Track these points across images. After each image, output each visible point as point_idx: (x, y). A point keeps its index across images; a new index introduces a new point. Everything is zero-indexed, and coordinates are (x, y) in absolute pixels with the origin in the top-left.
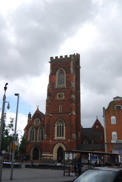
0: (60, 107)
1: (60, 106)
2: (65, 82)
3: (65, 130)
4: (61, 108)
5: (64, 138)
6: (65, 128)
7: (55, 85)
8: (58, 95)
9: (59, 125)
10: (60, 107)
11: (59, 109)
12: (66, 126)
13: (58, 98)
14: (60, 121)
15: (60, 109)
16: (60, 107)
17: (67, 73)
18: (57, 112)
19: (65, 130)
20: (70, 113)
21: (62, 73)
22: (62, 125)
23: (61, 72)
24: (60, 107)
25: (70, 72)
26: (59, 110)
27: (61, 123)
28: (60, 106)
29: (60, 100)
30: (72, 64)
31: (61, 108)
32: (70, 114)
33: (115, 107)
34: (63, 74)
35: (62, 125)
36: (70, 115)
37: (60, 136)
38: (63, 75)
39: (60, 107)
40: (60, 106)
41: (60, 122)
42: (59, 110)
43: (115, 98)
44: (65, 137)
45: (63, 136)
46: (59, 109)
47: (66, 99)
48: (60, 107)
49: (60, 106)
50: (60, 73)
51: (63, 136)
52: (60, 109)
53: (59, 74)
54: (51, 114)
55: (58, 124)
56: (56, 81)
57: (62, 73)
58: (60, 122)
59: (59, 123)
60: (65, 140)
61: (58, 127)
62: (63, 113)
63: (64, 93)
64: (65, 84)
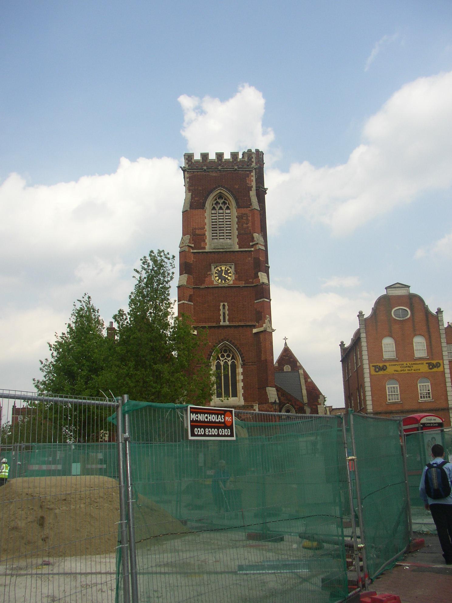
0: (224, 309)
1: (222, 304)
2: (236, 233)
3: (240, 377)
4: (227, 312)
5: (239, 400)
6: (240, 370)
7: (204, 241)
8: (214, 271)
9: (222, 363)
10: (224, 309)
11: (221, 313)
12: (243, 366)
13: (216, 280)
14: (225, 351)
15: (224, 314)
16: (221, 307)
17: (239, 206)
18: (214, 325)
19: (240, 377)
20: (254, 327)
21: (224, 203)
22: (230, 363)
23: (221, 201)
24: (221, 307)
25: (251, 204)
26: (222, 318)
27: (228, 356)
28: (224, 305)
29: (221, 287)
30: (254, 179)
31: (227, 312)
32: (255, 331)
33: (394, 310)
34: (228, 208)
35: (230, 363)
36: (255, 333)
37: (227, 395)
38: (228, 211)
39: (224, 308)
40: (224, 305)
41: (225, 355)
42: (222, 318)
43: (390, 287)
44: (242, 398)
45: (235, 395)
47: (242, 284)
48: (224, 308)
49: (222, 304)
50: (217, 203)
51: (235, 395)
52: (224, 314)
53: (214, 208)
54: (195, 328)
55: (218, 358)
56: (207, 227)
57: (224, 203)
58: (225, 355)
59: (223, 356)
60: (244, 407)
61: (218, 366)
62: (235, 327)
63: (233, 267)
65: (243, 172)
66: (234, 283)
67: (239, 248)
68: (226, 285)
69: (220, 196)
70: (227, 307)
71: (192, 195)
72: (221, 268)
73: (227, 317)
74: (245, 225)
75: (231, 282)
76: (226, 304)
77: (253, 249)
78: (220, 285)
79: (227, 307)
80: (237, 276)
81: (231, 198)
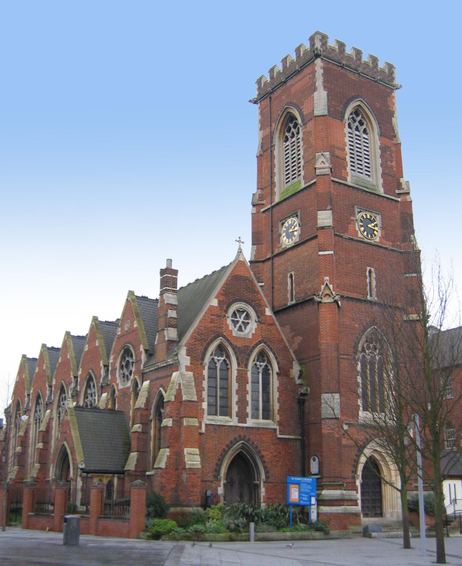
11: (368, 280)
18: (360, 297)
28: (370, 272)
40: (370, 272)
46: (368, 280)
59: (369, 348)
64: (381, 181)
65: (383, 88)
66: (380, 242)
67: (385, 193)
68: (372, 241)
69: (356, 112)
70: (374, 275)
71: (328, 94)
72: (366, 215)
73: (374, 290)
74: (389, 163)
75: (378, 240)
76: (373, 269)
77: (399, 200)
78: (366, 240)
79: (374, 275)
80: (384, 233)
81: (372, 119)
